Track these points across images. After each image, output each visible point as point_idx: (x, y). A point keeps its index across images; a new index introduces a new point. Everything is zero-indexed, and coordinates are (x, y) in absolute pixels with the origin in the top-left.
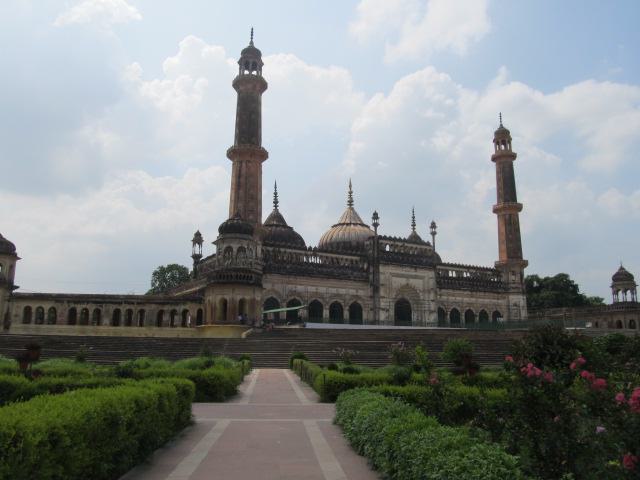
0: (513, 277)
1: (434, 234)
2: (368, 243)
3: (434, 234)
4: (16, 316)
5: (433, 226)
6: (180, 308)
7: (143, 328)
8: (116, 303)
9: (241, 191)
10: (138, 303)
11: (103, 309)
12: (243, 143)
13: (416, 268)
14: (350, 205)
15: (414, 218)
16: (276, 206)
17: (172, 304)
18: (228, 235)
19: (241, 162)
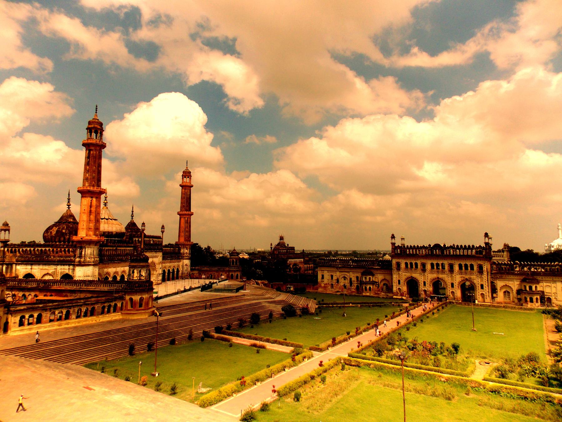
0: (186, 251)
1: (163, 232)
2: (137, 239)
3: (163, 232)
4: (15, 323)
5: (163, 227)
6: (113, 304)
7: (95, 317)
8: (77, 306)
9: (91, 216)
10: (92, 304)
11: (71, 311)
12: (93, 186)
13: (156, 252)
14: (105, 205)
15: (133, 211)
16: (69, 208)
17: (109, 302)
18: (141, 264)
19: (92, 197)
